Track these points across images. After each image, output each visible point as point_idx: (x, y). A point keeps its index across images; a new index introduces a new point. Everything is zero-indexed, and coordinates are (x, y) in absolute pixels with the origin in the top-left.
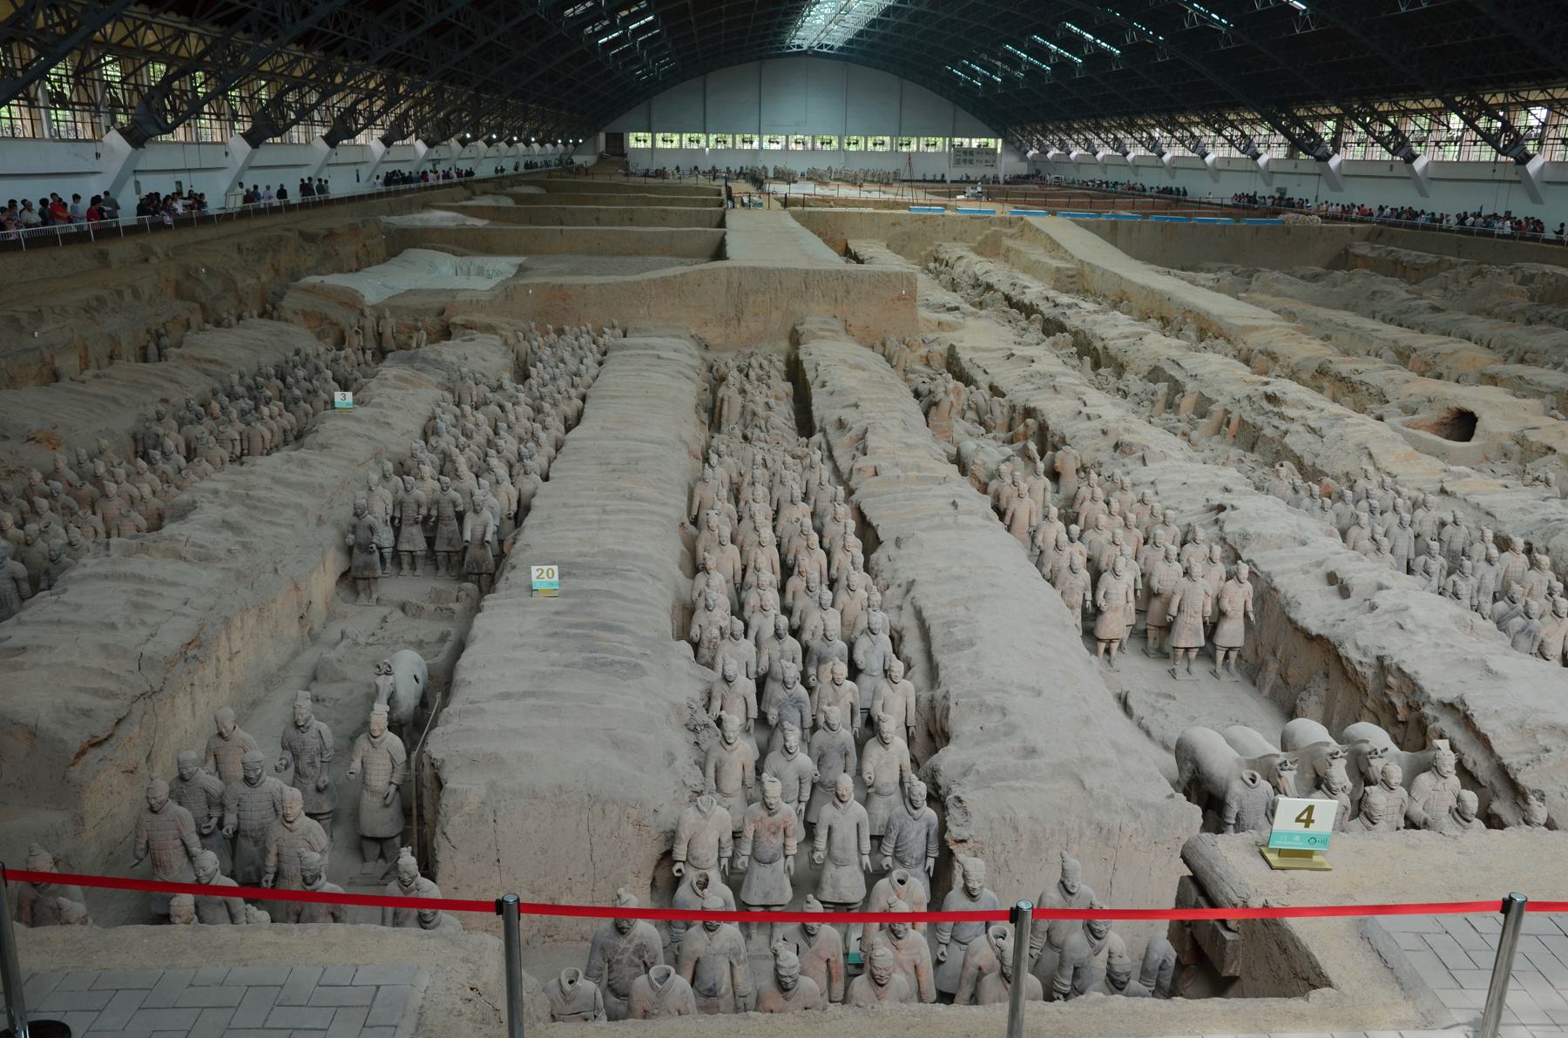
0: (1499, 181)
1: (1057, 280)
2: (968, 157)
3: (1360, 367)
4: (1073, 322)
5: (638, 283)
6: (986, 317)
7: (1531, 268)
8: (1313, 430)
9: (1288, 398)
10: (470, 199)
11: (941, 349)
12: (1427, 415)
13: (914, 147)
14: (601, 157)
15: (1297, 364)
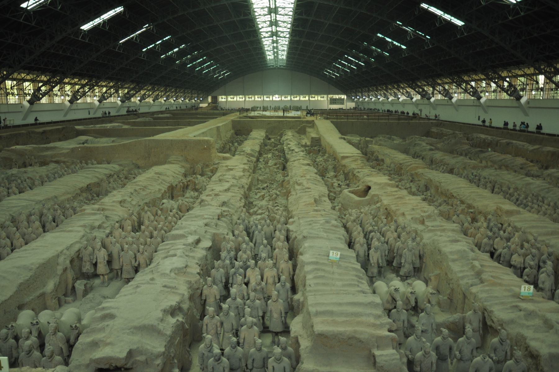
0: (476, 106)
1: (312, 142)
2: (335, 101)
3: (360, 170)
4: (288, 156)
5: (115, 146)
6: (243, 155)
7: (475, 135)
8: (296, 194)
9: (299, 182)
10: (136, 119)
11: (216, 166)
12: (361, 187)
13: (316, 99)
14: (209, 104)
15: (350, 170)
